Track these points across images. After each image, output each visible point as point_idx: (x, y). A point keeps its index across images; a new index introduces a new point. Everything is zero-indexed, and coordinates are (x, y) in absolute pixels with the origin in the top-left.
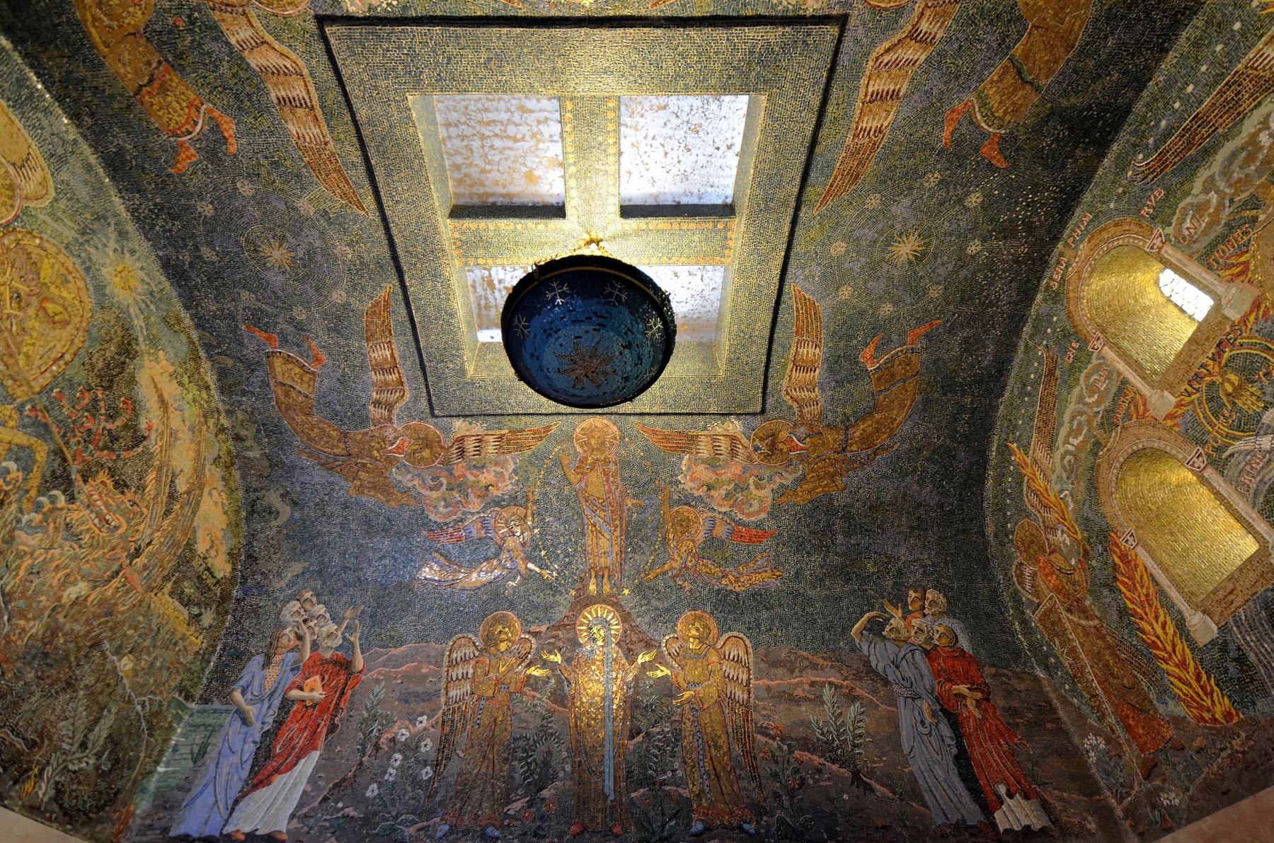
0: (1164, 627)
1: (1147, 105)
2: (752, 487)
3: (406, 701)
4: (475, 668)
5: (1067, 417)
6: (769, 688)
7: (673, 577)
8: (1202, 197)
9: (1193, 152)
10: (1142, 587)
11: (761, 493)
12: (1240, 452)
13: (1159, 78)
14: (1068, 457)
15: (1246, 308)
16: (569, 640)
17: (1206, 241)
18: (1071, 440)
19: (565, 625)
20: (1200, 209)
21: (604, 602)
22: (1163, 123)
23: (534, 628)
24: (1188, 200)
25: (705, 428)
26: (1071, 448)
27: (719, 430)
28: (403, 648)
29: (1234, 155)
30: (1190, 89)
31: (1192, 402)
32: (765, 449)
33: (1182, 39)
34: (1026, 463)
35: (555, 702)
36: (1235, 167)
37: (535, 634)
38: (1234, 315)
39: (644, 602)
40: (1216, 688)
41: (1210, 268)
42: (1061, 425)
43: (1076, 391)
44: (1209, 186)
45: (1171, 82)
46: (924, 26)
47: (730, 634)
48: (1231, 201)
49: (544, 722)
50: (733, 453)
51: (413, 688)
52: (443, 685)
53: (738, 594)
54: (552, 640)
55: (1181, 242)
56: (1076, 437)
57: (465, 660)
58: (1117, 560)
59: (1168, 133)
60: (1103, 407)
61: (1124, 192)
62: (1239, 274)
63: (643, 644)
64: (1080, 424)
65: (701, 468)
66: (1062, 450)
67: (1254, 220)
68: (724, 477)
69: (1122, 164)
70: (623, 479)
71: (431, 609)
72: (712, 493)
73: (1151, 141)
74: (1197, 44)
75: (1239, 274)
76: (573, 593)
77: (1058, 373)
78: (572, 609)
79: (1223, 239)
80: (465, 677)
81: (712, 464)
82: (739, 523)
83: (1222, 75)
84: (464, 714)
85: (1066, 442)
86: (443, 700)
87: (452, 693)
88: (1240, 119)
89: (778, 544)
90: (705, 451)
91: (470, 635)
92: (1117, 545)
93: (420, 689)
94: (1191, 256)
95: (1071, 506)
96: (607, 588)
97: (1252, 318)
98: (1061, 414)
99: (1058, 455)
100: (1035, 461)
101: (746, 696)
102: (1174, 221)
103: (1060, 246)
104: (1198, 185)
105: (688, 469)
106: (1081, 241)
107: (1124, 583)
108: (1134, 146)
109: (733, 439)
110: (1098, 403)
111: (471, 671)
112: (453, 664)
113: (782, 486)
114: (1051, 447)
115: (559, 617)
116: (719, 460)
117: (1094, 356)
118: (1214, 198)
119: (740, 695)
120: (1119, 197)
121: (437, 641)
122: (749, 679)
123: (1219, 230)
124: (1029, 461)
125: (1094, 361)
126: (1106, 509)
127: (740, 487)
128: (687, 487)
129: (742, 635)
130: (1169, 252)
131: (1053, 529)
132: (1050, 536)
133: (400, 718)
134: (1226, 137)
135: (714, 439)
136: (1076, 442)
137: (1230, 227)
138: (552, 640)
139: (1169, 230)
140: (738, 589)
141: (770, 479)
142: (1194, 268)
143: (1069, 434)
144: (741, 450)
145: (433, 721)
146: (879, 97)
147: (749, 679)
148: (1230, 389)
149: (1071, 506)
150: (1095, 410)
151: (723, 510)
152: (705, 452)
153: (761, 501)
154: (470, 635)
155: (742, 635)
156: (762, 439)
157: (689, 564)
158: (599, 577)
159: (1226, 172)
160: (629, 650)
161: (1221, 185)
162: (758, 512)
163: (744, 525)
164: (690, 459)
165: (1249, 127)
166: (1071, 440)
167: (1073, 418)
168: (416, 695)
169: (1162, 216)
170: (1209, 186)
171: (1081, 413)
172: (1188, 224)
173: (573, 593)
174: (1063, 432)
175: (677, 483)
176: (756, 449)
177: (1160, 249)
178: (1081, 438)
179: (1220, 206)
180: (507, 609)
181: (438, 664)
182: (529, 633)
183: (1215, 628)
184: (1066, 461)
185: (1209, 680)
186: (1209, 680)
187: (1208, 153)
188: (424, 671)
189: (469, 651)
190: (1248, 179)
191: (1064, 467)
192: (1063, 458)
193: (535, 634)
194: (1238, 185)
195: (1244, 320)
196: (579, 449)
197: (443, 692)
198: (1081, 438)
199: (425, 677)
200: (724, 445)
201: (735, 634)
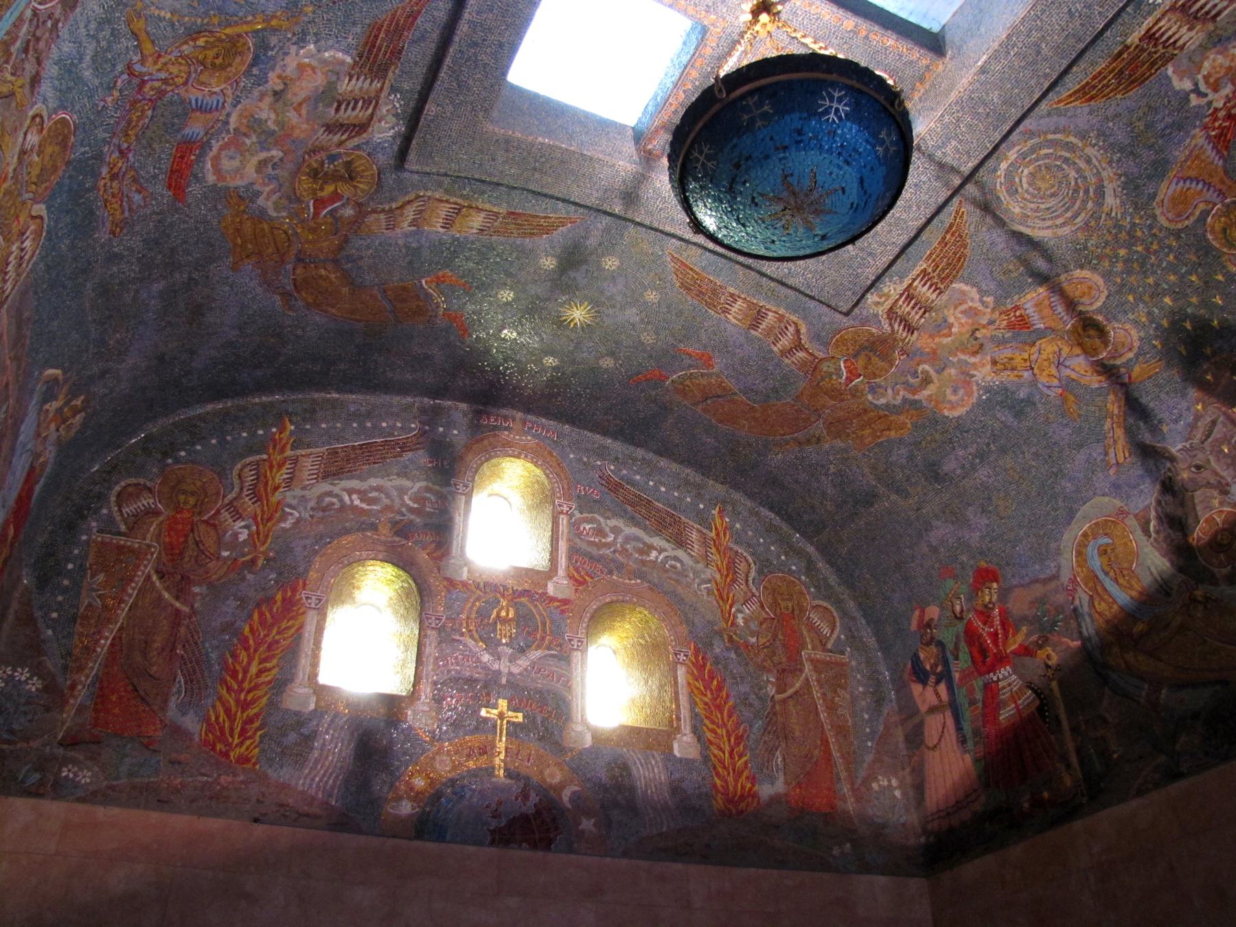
0: (260, 672)
1: (644, 459)
5: (373, 482)
8: (607, 529)
9: (629, 508)
10: (279, 633)
12: (465, 645)
13: (663, 463)
14: (335, 500)
15: (560, 596)
17: (584, 546)
18: (354, 497)
20: (600, 532)
22: (638, 477)
24: (602, 520)
26: (346, 498)
29: (637, 539)
30: (663, 489)
31: (473, 592)
33: (688, 471)
34: (283, 450)
36: (633, 543)
38: (551, 590)
40: (257, 738)
41: (569, 558)
42: (361, 478)
43: (406, 483)
44: (616, 531)
45: (661, 471)
46: (801, 354)
48: (615, 551)
55: (575, 526)
56: (362, 501)
58: (279, 597)
59: (633, 483)
60: (412, 517)
61: (585, 464)
62: (576, 580)
64: (372, 501)
65: (320, 80)
66: (336, 490)
67: (611, 573)
69: (602, 453)
72: (268, 100)
73: (625, 472)
74: (687, 483)
75: (576, 580)
77: (410, 454)
79: (591, 558)
81: (327, 95)
82: (205, 146)
83: (675, 508)
85: (350, 492)
88: (658, 533)
92: (294, 590)
94: (569, 540)
95: (286, 525)
97: (557, 604)
98: (371, 474)
99: (325, 487)
100: (296, 461)
102: (585, 515)
103: (519, 415)
104: (613, 522)
106: (533, 436)
107: (261, 614)
108: (617, 458)
110: (411, 510)
113: (258, 194)
114: (326, 475)
116: (330, 105)
117: (448, 489)
118: (610, 539)
120: (580, 460)
123: (595, 552)
124: (289, 453)
125: (445, 490)
126: (317, 562)
128: (288, 59)
130: (563, 520)
131: (237, 515)
132: (225, 515)
134: (645, 529)
136: (357, 502)
137: (600, 559)
139: (578, 515)
142: (563, 546)
143: (359, 492)
146: (759, 315)
148: (503, 614)
149: (286, 525)
150: (404, 509)
159: (628, 539)
161: (620, 540)
162: (218, 171)
164: (343, 63)
165: (657, 541)
166: (354, 497)
167: (378, 489)
169: (586, 504)
170: (616, 531)
171: (388, 496)
172: (587, 527)
174: (354, 484)
175: (301, 41)
177: (562, 512)
178: (364, 506)
179: (607, 545)
183: (312, 707)
184: (327, 499)
185: (258, 729)
186: (258, 729)
187: (633, 521)
190: (629, 556)
191: (320, 498)
192: (330, 494)
194: (624, 551)
195: (552, 599)
198: (364, 506)
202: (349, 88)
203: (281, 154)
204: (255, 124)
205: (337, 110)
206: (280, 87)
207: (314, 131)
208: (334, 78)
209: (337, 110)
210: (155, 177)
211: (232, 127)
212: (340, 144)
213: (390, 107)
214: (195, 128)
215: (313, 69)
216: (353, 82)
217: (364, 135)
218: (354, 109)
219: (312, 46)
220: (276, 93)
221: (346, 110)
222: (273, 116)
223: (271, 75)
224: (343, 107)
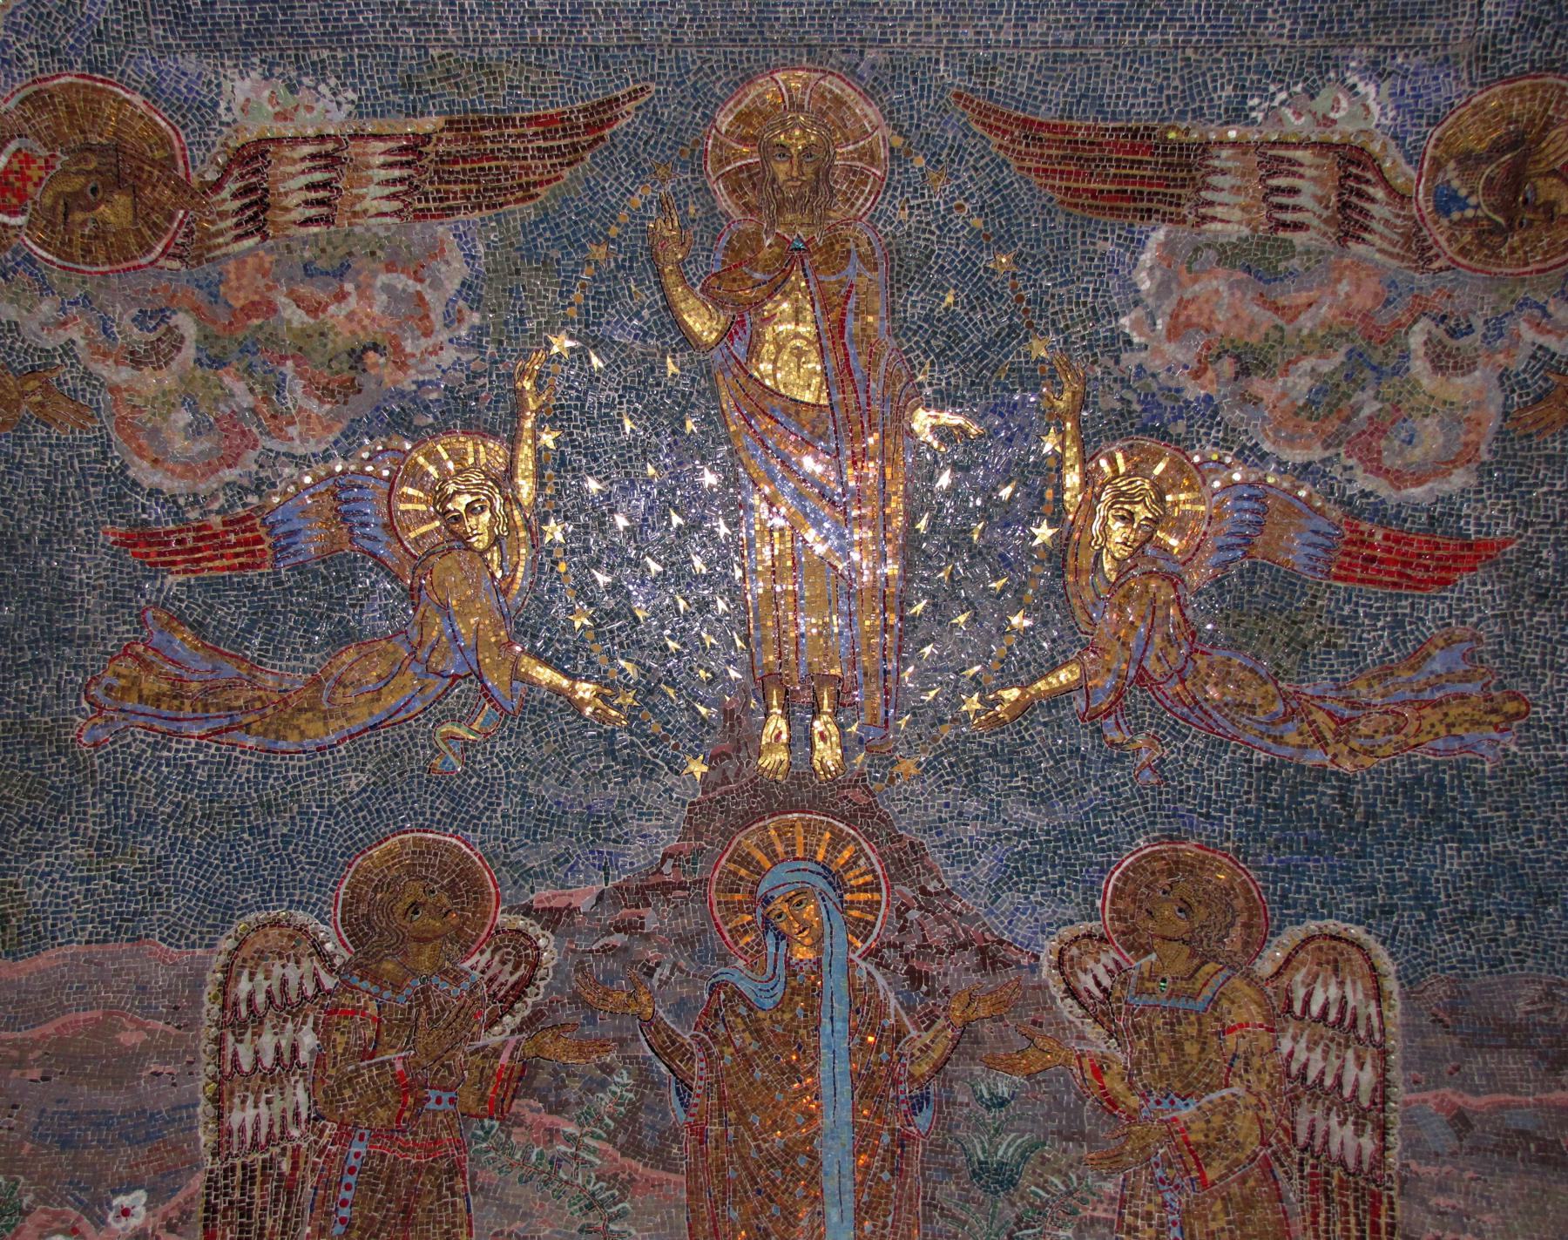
2: (1419, 366)
3: (65, 1143)
4: (324, 1031)
6: (1460, 1121)
7: (1091, 716)
11: (1460, 387)
16: (684, 941)
19: (666, 888)
21: (816, 803)
23: (543, 895)
25: (1238, 114)
27: (1296, 124)
28: (48, 959)
32: (1479, 205)
35: (633, 1149)
37: (553, 918)
39: (972, 805)
47: (1312, 926)
49: (593, 1219)
50: (1349, 221)
51: (87, 1095)
52: (203, 1085)
53: (1347, 781)
54: (618, 939)
57: (286, 1006)
63: (970, 958)
68: (1306, 322)
70: (901, 330)
71: (147, 821)
76: (698, 768)
78: (693, 829)
80: (287, 1061)
81: (1259, 262)
84: (289, 1186)
86: (205, 1138)
87: (242, 1116)
89: (1514, 595)
90: (1231, 221)
91: (301, 916)
93: (115, 1100)
96: (827, 754)
101: (1368, 1144)
105: (1163, 289)
109: (1352, 162)
111: (308, 1040)
112: (239, 1020)
115: (636, 857)
116: (1288, 249)
119: (1344, 1137)
121: (174, 935)
122: (1383, 1084)
127: (1370, 352)
128: (1155, 365)
129: (1356, 931)
133: (43, 1198)
135: (1272, 160)
138: (618, 939)
140: (1347, 766)
141: (1496, 327)
144: (1380, 209)
145: (171, 1207)
147: (1383, 1084)
151: (1297, 456)
152: (1231, 221)
153: (1455, 417)
154: (301, 916)
155: (1356, 931)
156: (1468, 161)
157: (1150, 664)
158: (800, 710)
160: (916, 977)
162: (1441, 468)
163: (1378, 512)
164: (1168, 245)
168: (101, 1119)
173: (698, 768)
176: (1446, 202)
180: (441, 826)
181: (182, 1014)
182: (527, 911)
188: (131, 1038)
189: (298, 974)
193: (553, 918)
196: (725, 202)
197: (204, 1109)
199: (130, 1061)
200: (1311, 189)
201: (1332, 925)
202: (1237, 214)
203: (1424, 324)
204: (1327, 401)
205: (1298, 226)
206: (1227, 367)
207: (1359, 263)
208: (1211, 254)
209: (1298, 226)
210: (1398, 623)
211: (1317, 454)
212: (1399, 197)
213: (1288, 112)
214: (1296, 549)
215: (1183, 304)
216: (1219, 211)
217: (1375, 147)
218: (1293, 191)
219: (1124, 321)
220: (1244, 371)
221: (1296, 208)
222: (1306, 364)
223: (1193, 391)
224: (1288, 217)
